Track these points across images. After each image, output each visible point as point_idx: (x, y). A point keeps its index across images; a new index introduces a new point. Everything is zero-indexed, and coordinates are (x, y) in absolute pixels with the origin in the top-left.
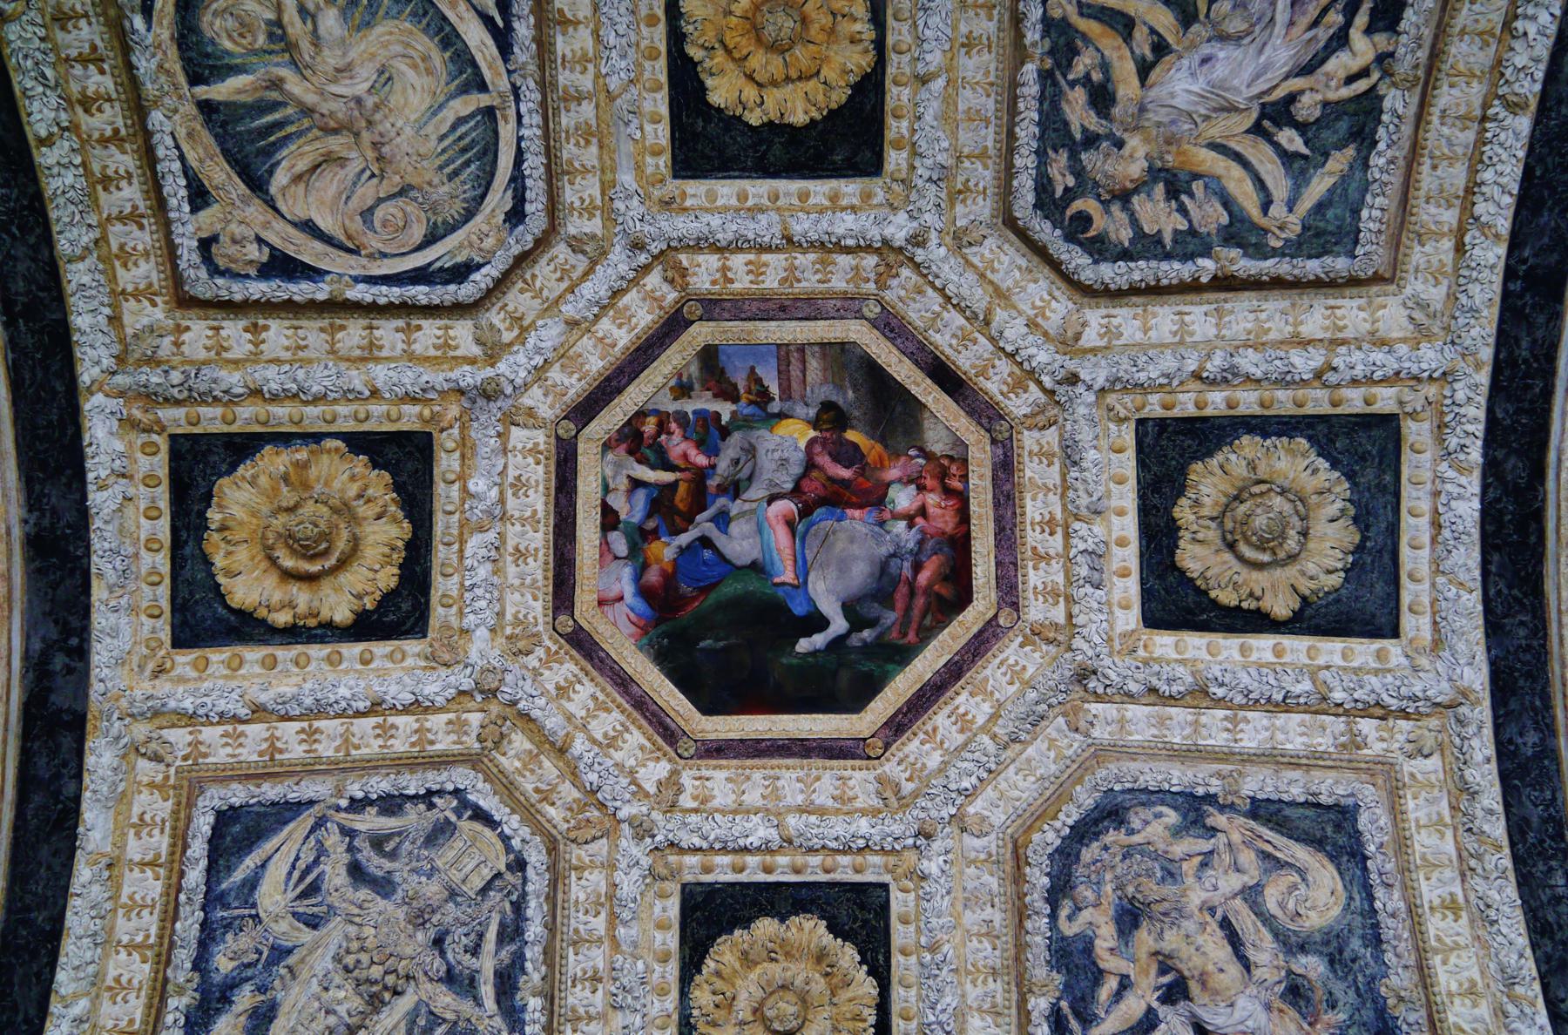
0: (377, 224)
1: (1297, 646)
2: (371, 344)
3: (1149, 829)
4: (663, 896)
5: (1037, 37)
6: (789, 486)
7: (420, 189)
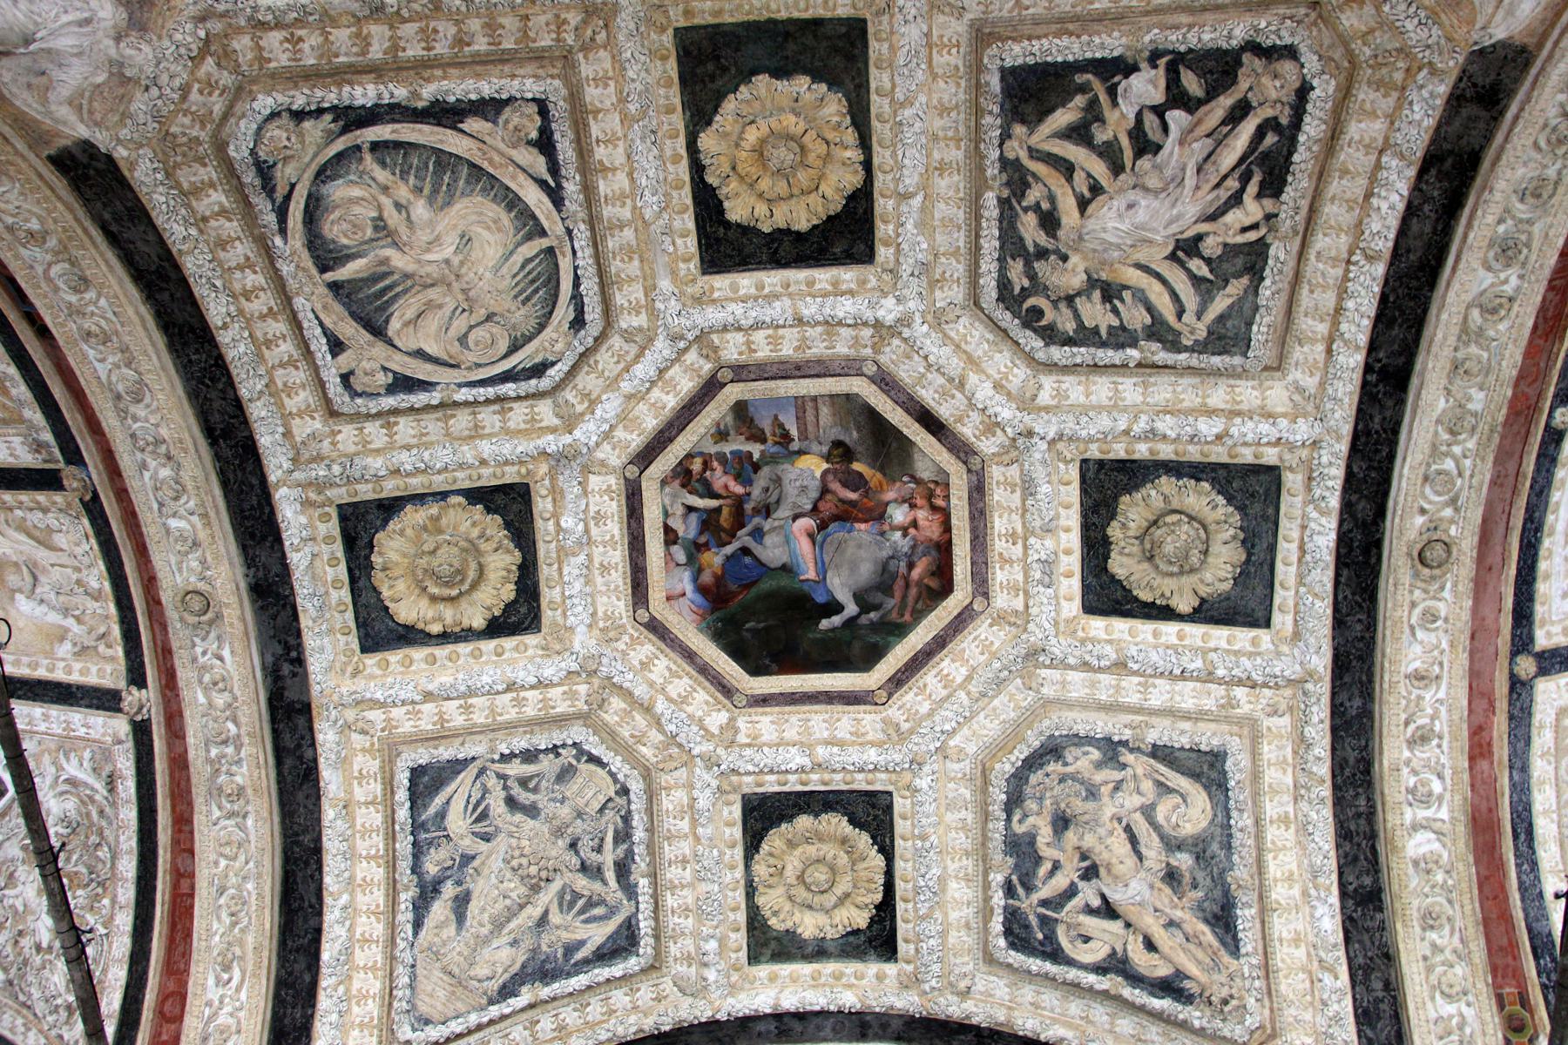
0: (471, 344)
1: (1195, 631)
2: (476, 426)
3: (1079, 763)
4: (729, 804)
5: (996, 172)
6: (809, 507)
7: (502, 316)
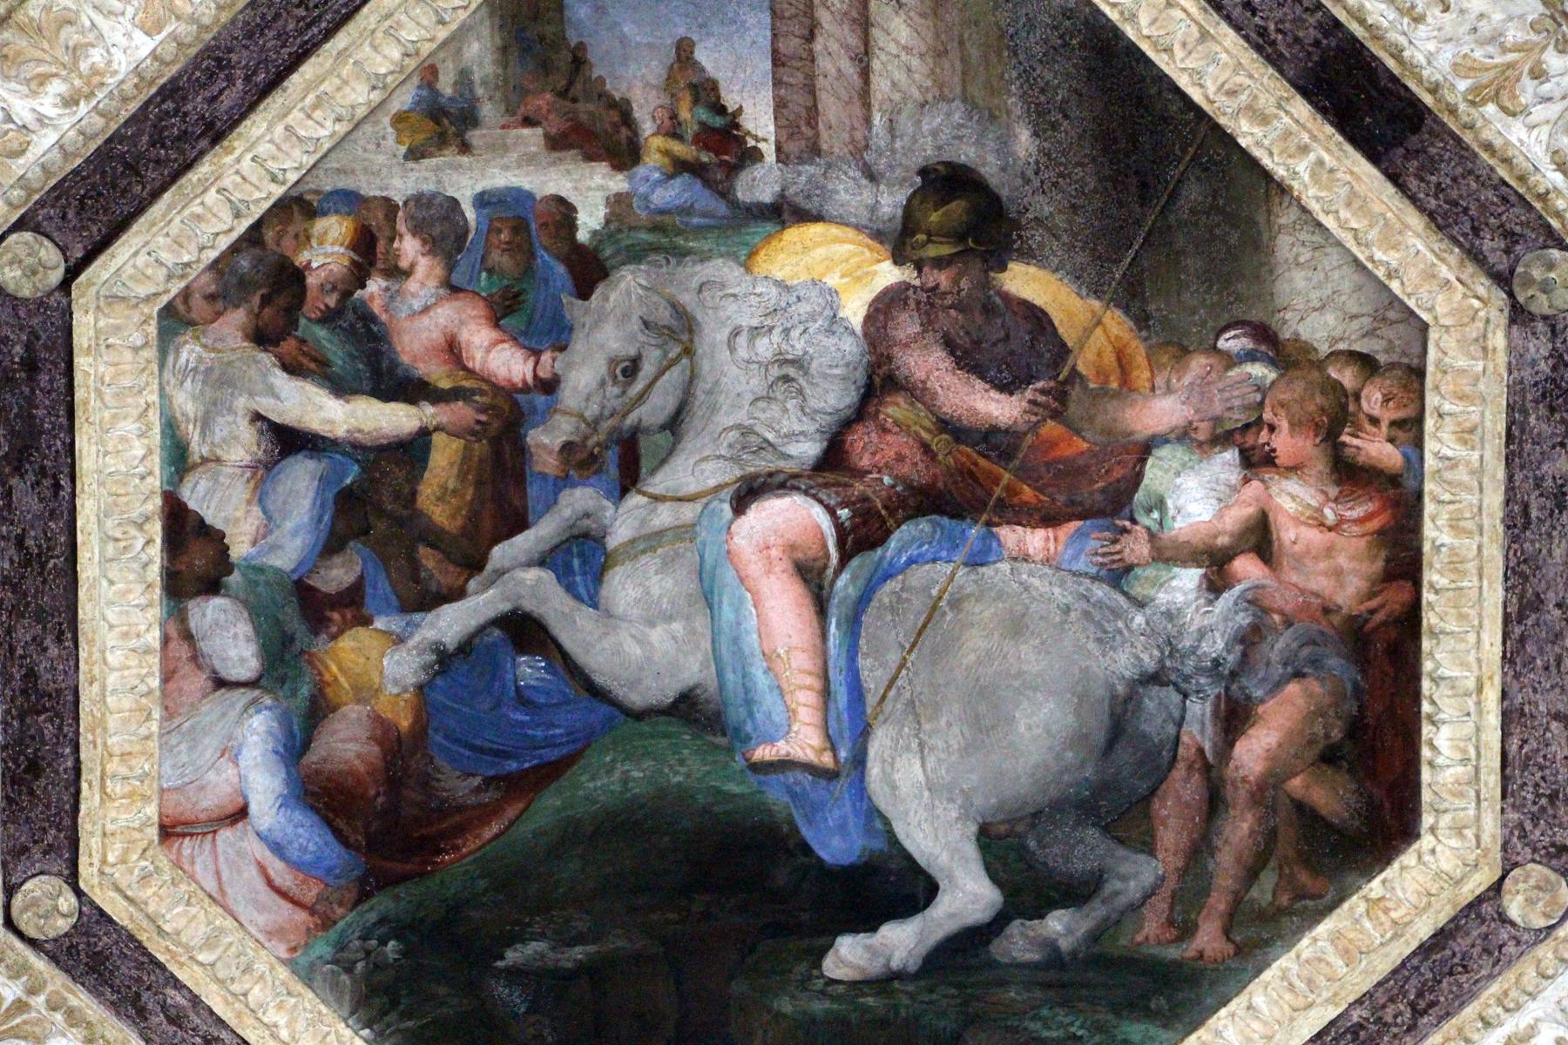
6: (808, 449)
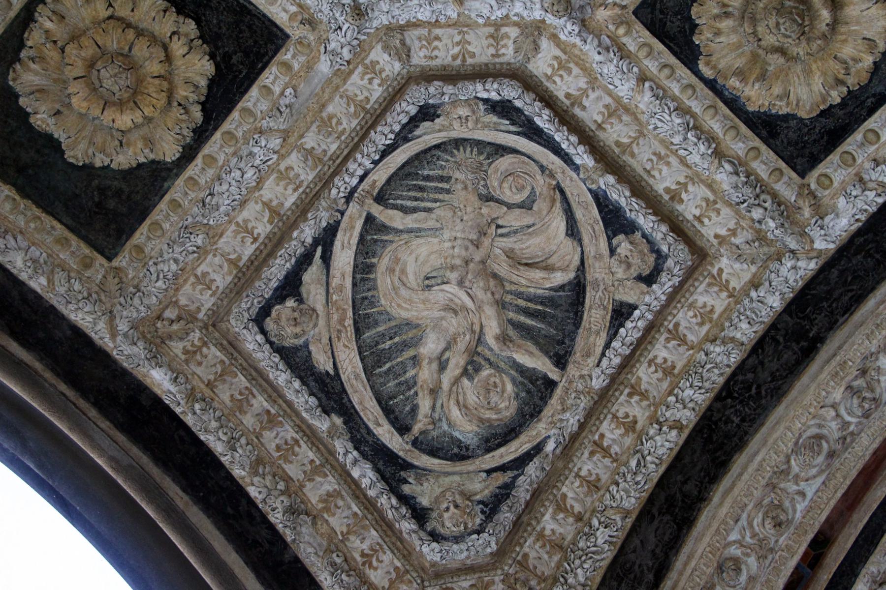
0: (526, 193)
2: (610, 115)
7: (476, 189)
